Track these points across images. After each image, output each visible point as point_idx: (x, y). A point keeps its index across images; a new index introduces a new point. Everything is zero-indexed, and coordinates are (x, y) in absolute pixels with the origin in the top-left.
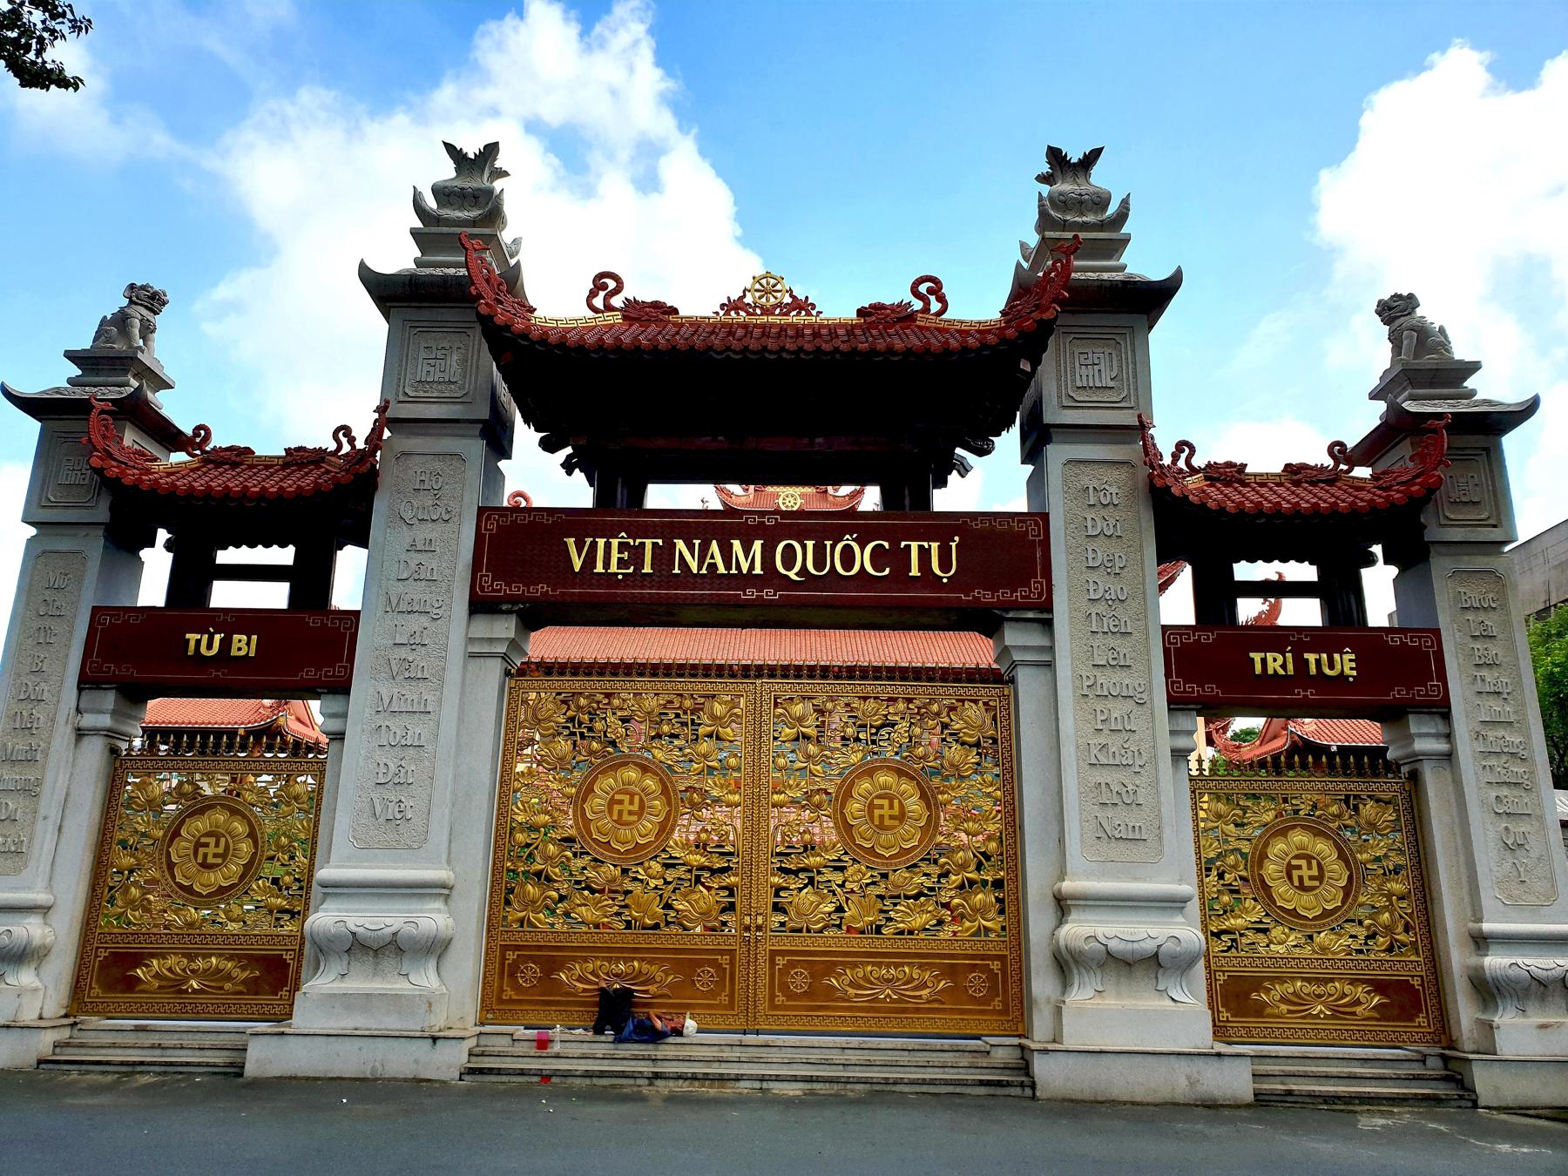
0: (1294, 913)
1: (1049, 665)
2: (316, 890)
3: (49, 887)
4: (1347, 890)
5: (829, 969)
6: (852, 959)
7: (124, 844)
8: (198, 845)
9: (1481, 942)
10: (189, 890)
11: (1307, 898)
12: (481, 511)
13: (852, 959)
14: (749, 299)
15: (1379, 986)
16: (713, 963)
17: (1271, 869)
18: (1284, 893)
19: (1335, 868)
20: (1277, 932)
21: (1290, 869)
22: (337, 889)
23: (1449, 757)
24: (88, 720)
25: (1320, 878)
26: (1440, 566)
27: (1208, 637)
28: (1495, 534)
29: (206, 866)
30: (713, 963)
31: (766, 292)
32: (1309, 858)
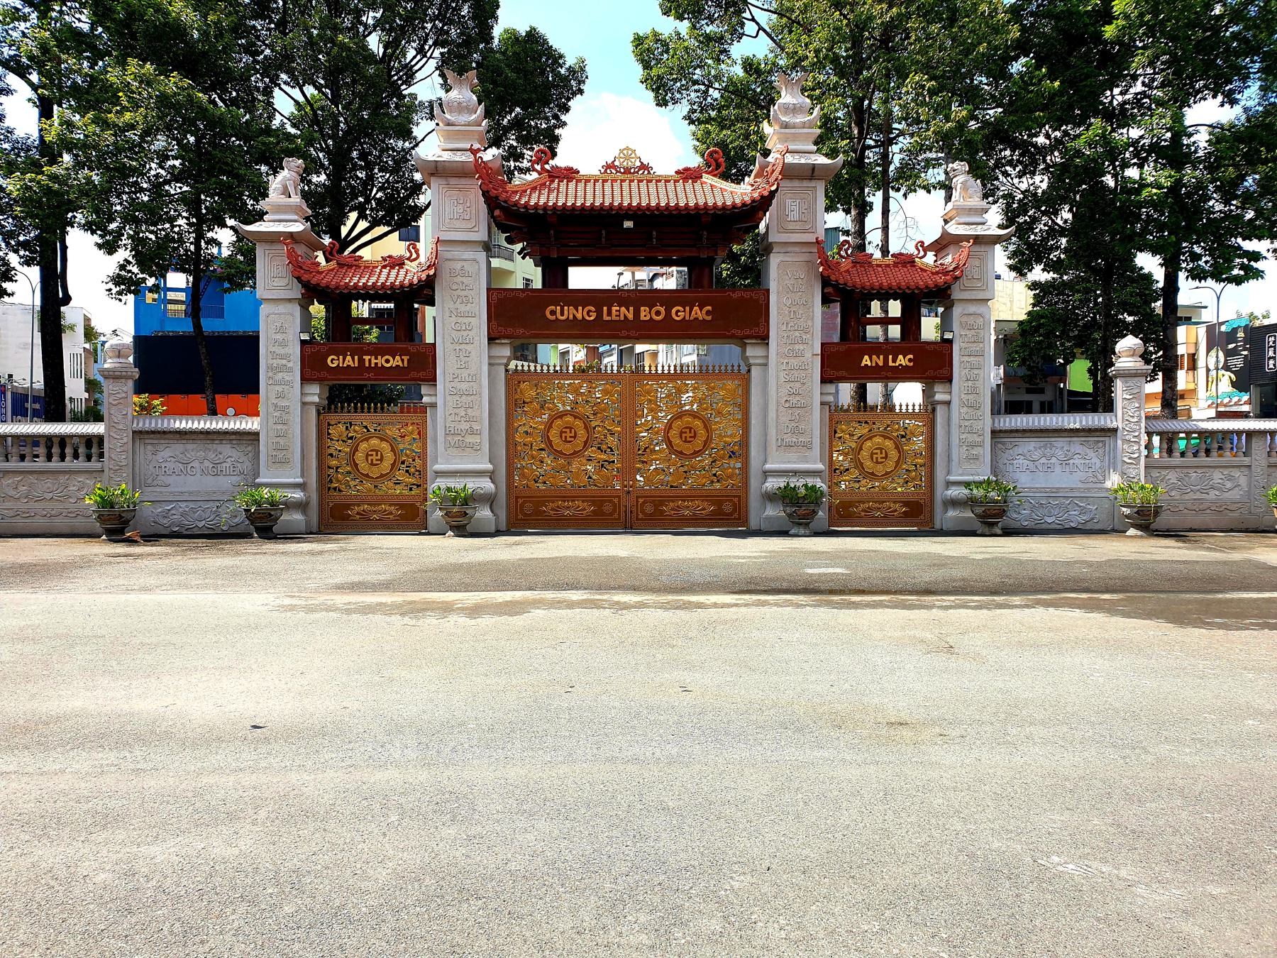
0: (872, 474)
1: (766, 365)
2: (430, 474)
3: (302, 476)
4: (897, 463)
5: (662, 503)
6: (674, 498)
7: (331, 455)
8: (367, 455)
9: (949, 484)
10: (367, 475)
11: (880, 467)
12: (488, 290)
13: (674, 498)
14: (617, 163)
15: (906, 504)
16: (610, 501)
17: (864, 453)
18: (868, 464)
19: (894, 454)
20: (864, 482)
21: (872, 454)
22: (440, 474)
23: (948, 403)
24: (309, 399)
25: (886, 457)
26: (957, 311)
27: (843, 348)
28: (980, 296)
29: (372, 464)
30: (610, 501)
31: (627, 158)
32: (881, 449)
